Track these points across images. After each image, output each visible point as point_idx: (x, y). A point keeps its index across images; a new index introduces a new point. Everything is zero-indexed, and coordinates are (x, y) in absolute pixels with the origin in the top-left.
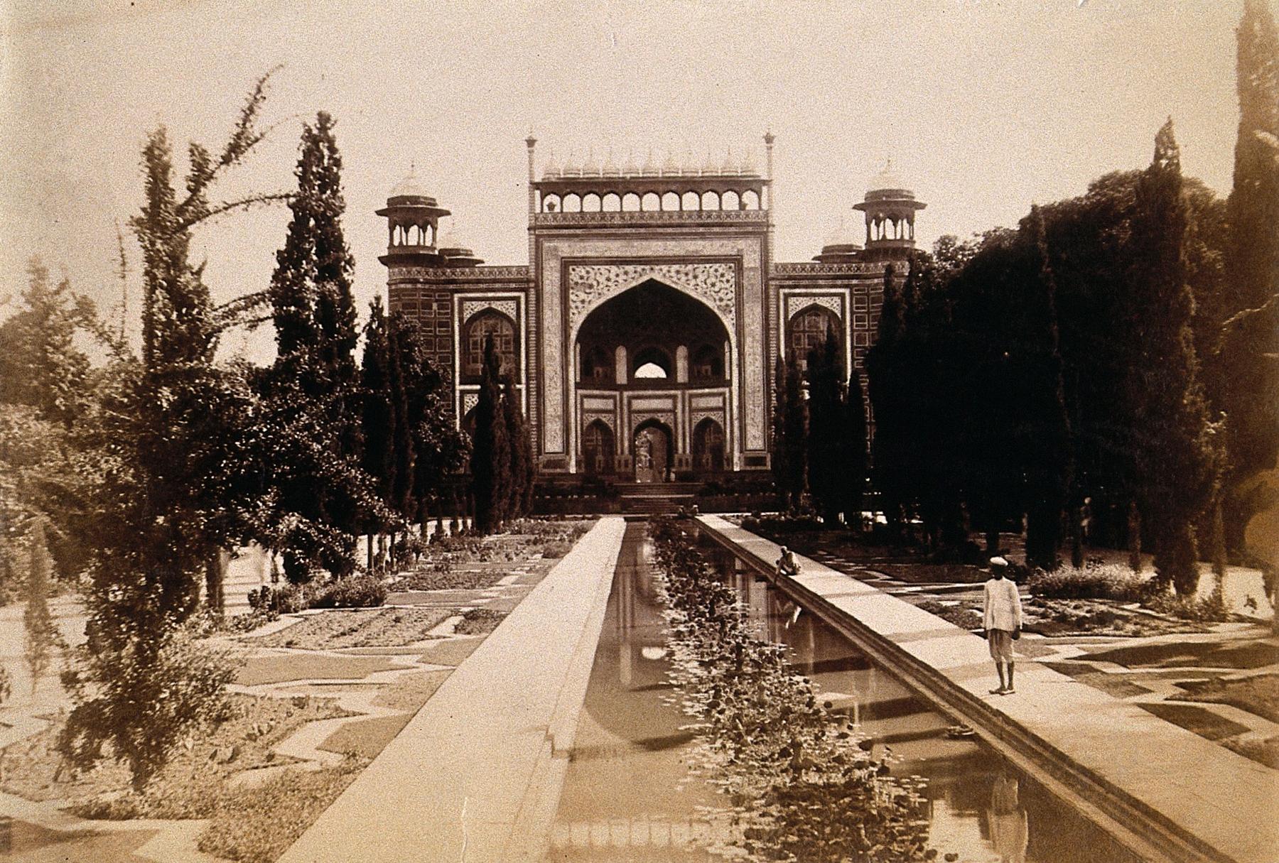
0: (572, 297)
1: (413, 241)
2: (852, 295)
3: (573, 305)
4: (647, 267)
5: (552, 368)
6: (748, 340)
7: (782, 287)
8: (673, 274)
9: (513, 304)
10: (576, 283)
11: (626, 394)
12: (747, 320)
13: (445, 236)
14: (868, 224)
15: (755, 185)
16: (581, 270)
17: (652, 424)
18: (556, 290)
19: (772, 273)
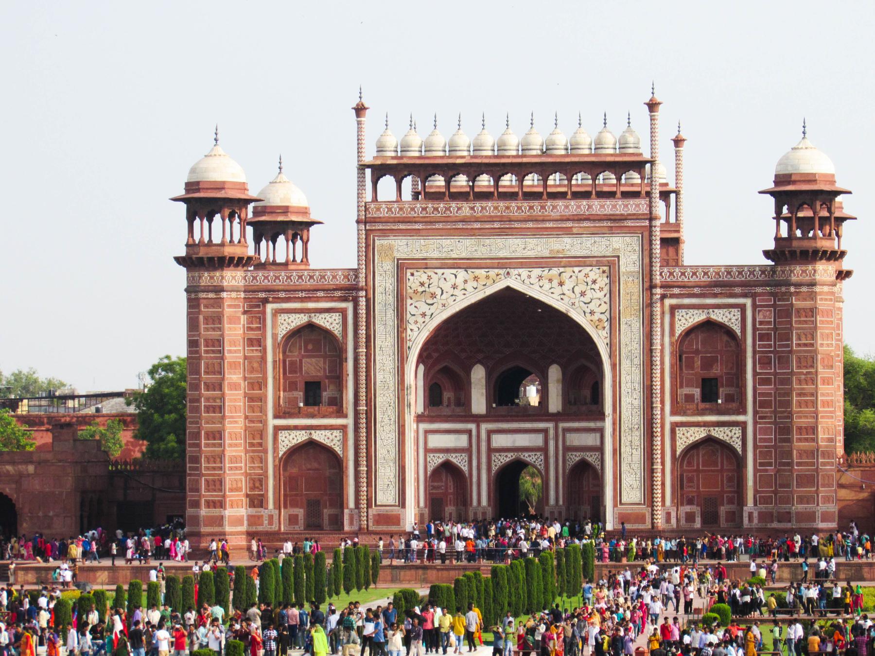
0: (410, 309)
2: (754, 306)
3: (412, 320)
4: (501, 271)
5: (385, 399)
6: (625, 365)
7: (673, 296)
8: (534, 280)
9: (337, 317)
10: (416, 292)
11: (484, 427)
15: (638, 166)
16: (422, 275)
18: (391, 299)
19: (658, 280)
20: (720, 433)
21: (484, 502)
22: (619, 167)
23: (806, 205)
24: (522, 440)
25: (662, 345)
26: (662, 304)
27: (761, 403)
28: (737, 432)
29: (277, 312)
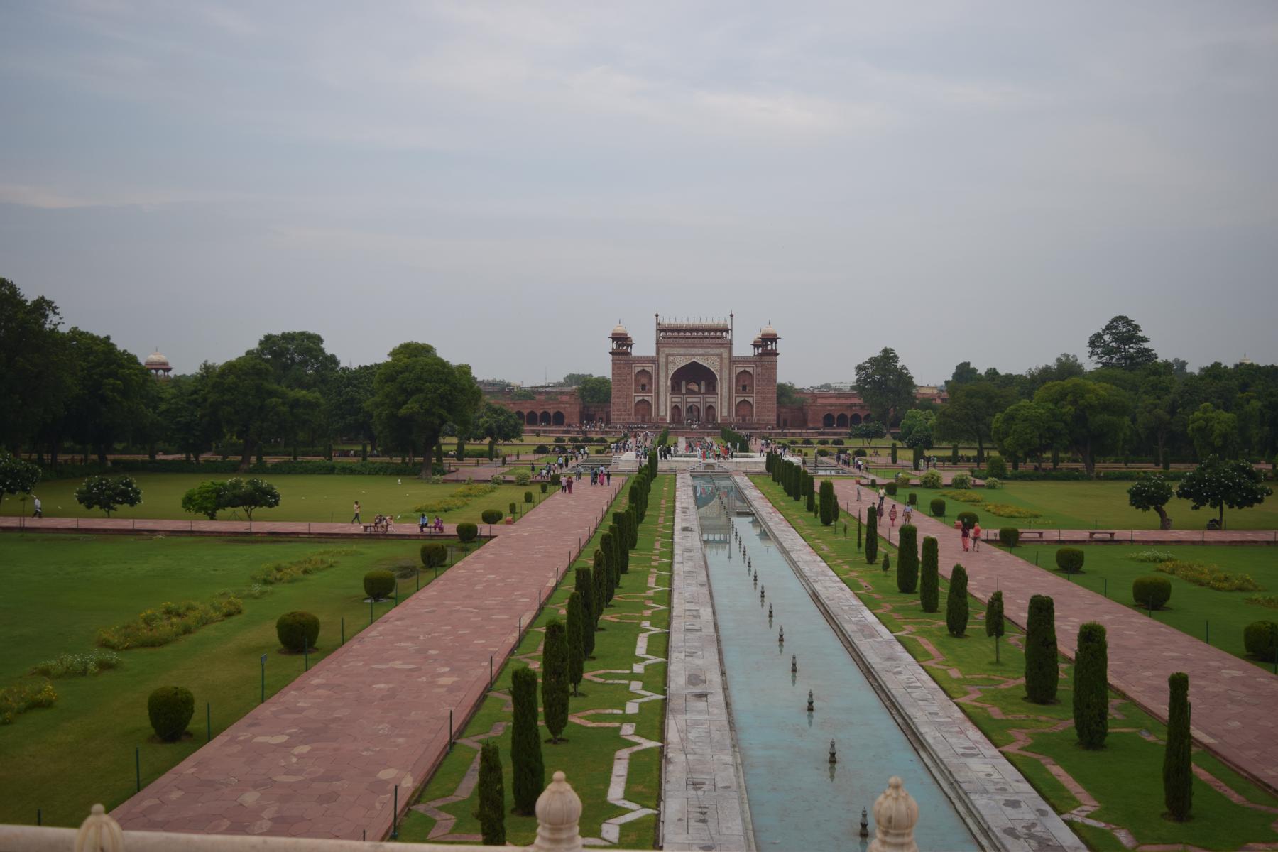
5: (662, 389)
22: (722, 331)
23: (767, 342)
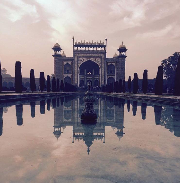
0: (79, 62)
1: (57, 53)
5: (76, 72)
6: (102, 68)
9: (71, 63)
11: (86, 76)
12: (102, 66)
13: (61, 53)
14: (119, 53)
17: (89, 80)
18: (77, 61)
20: (112, 77)
21: (86, 84)
24: (90, 78)
25: (106, 66)
26: (106, 62)
27: (117, 73)
28: (114, 76)
29: (64, 62)
